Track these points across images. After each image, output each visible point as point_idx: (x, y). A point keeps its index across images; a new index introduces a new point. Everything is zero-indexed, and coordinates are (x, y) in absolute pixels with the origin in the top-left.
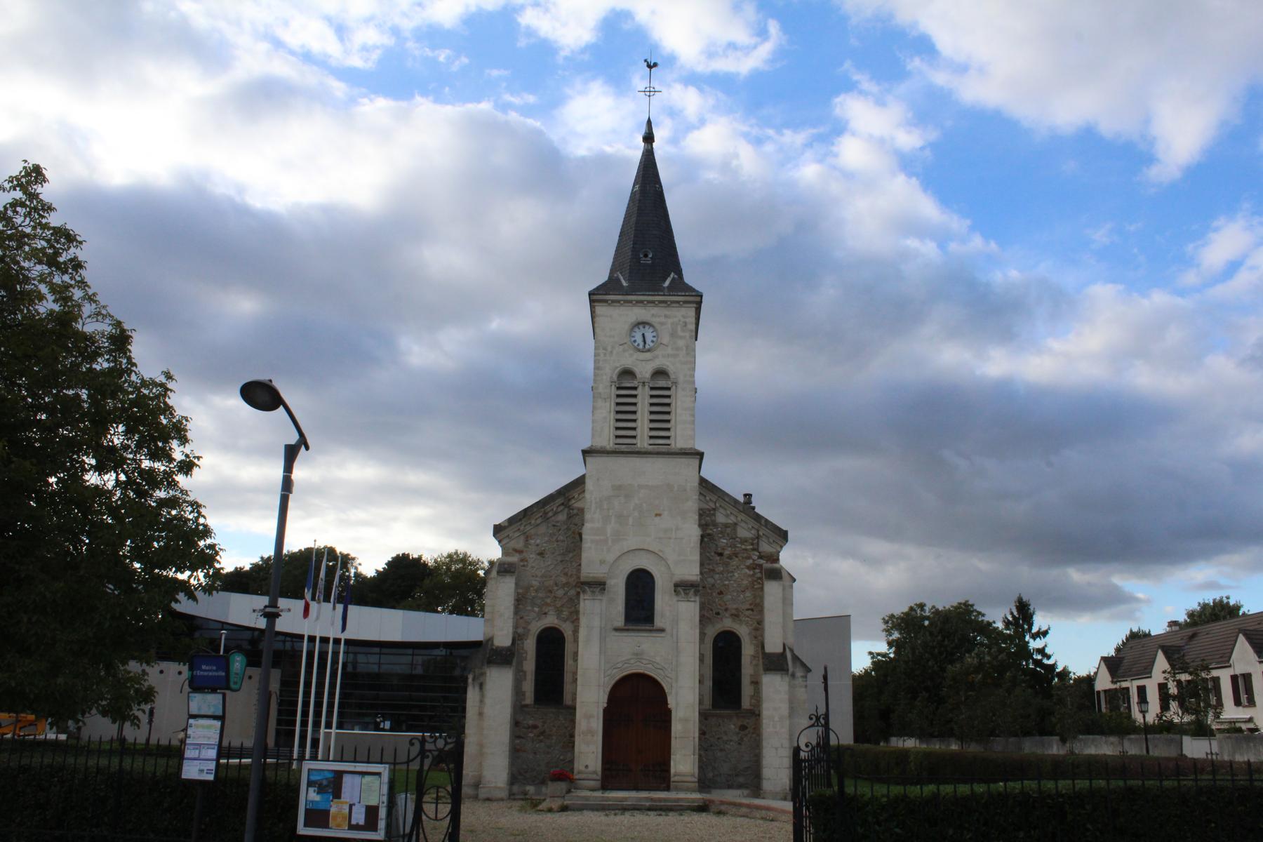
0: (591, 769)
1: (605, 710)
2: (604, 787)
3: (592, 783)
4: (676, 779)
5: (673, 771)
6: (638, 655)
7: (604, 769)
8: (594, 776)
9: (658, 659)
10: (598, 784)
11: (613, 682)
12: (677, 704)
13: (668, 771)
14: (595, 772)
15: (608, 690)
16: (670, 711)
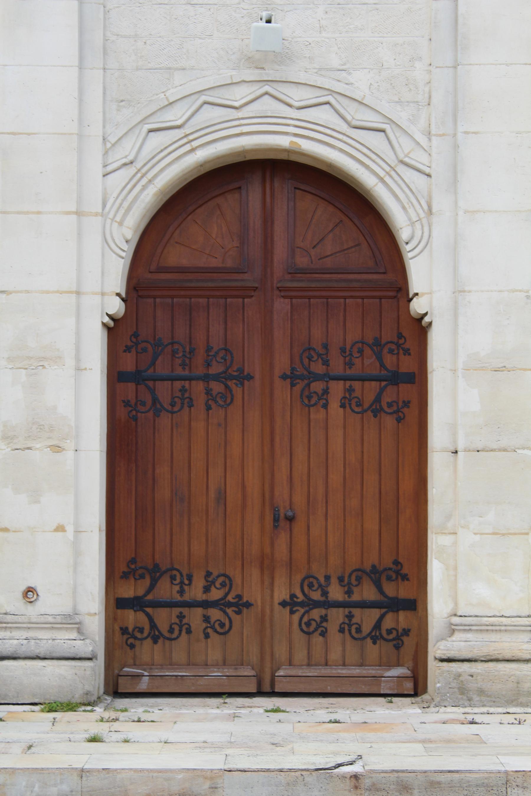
0: (51, 604)
1: (114, 329)
2: (123, 680)
3: (54, 676)
4: (456, 645)
5: (439, 605)
6: (267, 67)
7: (117, 604)
8: (66, 640)
9: (361, 83)
10: (90, 676)
11: (147, 198)
12: (459, 291)
13: (415, 604)
14: (72, 622)
15: (128, 229)
16: (420, 328)
